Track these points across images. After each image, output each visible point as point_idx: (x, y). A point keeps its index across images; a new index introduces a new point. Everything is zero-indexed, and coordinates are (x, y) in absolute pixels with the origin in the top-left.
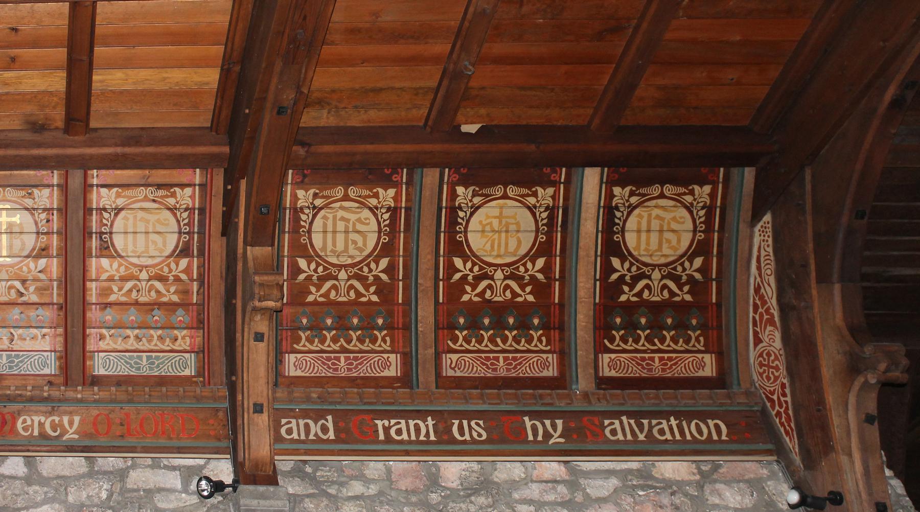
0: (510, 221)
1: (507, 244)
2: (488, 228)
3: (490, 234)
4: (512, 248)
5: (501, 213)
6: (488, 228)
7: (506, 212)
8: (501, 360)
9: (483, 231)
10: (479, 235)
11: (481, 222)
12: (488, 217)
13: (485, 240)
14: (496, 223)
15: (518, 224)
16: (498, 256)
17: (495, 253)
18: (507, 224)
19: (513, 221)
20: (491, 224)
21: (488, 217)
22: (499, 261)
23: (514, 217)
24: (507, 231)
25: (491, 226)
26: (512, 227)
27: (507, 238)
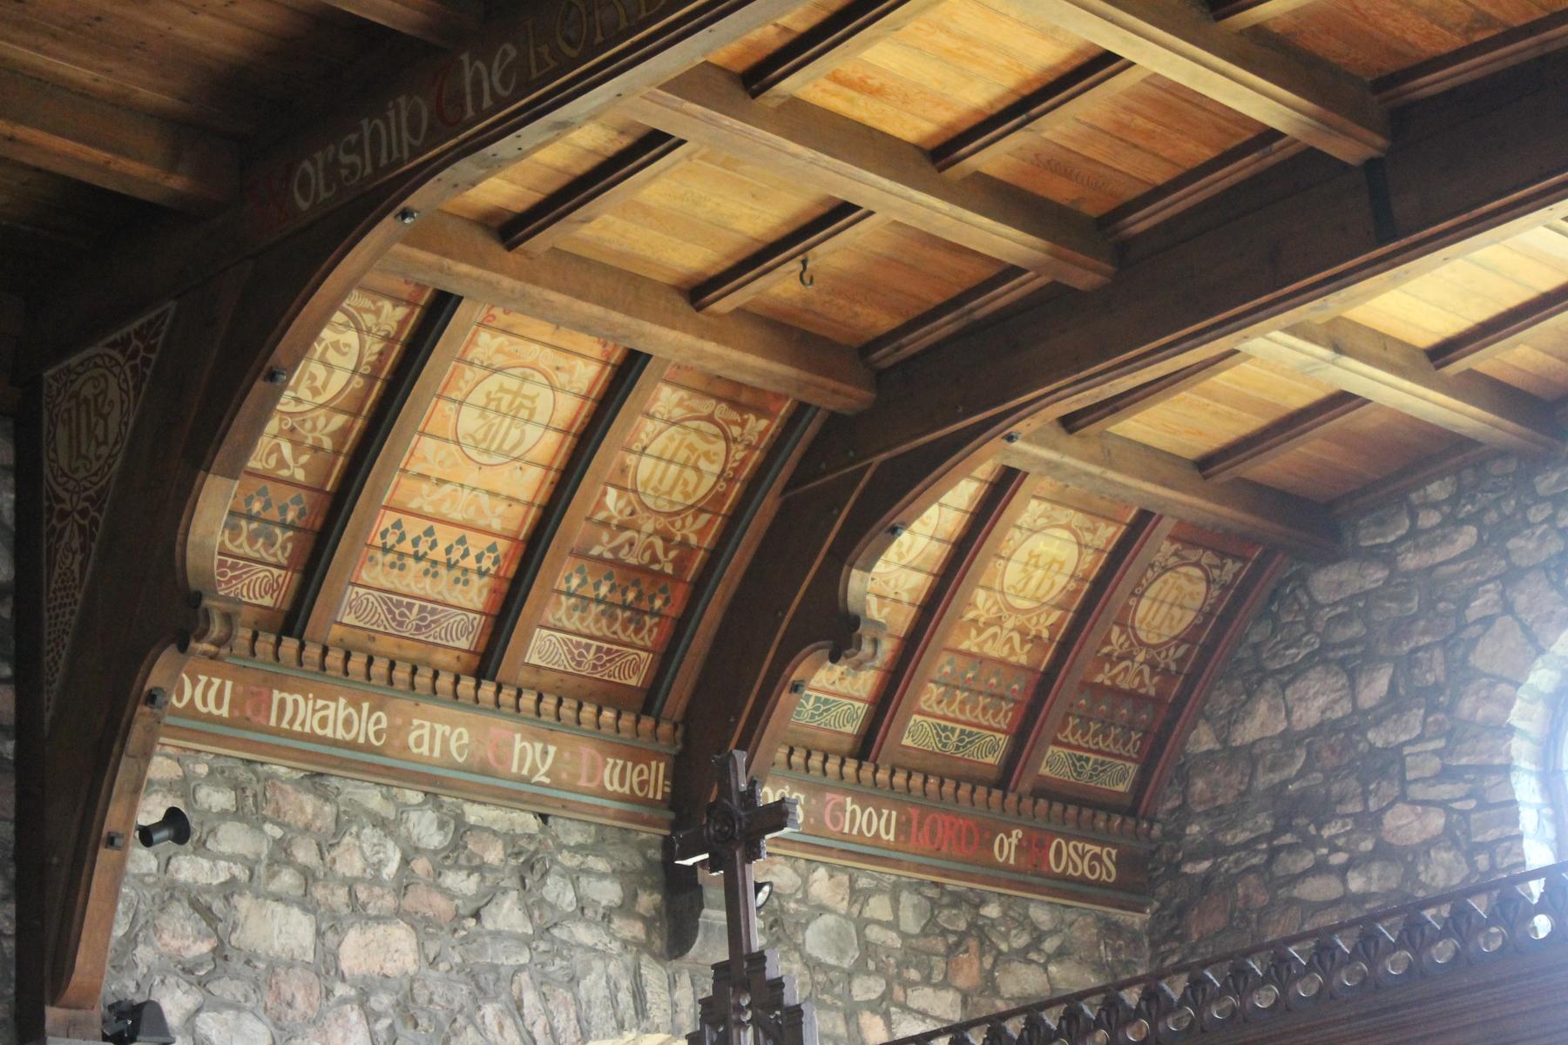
0: (527, 403)
1: (506, 434)
2: (493, 405)
3: (492, 415)
4: (506, 447)
5: (520, 388)
6: (493, 405)
7: (528, 389)
8: (415, 610)
9: (485, 408)
10: (477, 412)
11: (489, 394)
12: (502, 389)
13: (481, 422)
14: (507, 398)
15: (532, 412)
16: (487, 451)
17: (484, 446)
18: (521, 406)
19: (527, 403)
20: (500, 399)
21: (502, 389)
22: (484, 459)
23: (532, 399)
24: (514, 417)
25: (499, 405)
26: (524, 414)
27: (509, 428)
